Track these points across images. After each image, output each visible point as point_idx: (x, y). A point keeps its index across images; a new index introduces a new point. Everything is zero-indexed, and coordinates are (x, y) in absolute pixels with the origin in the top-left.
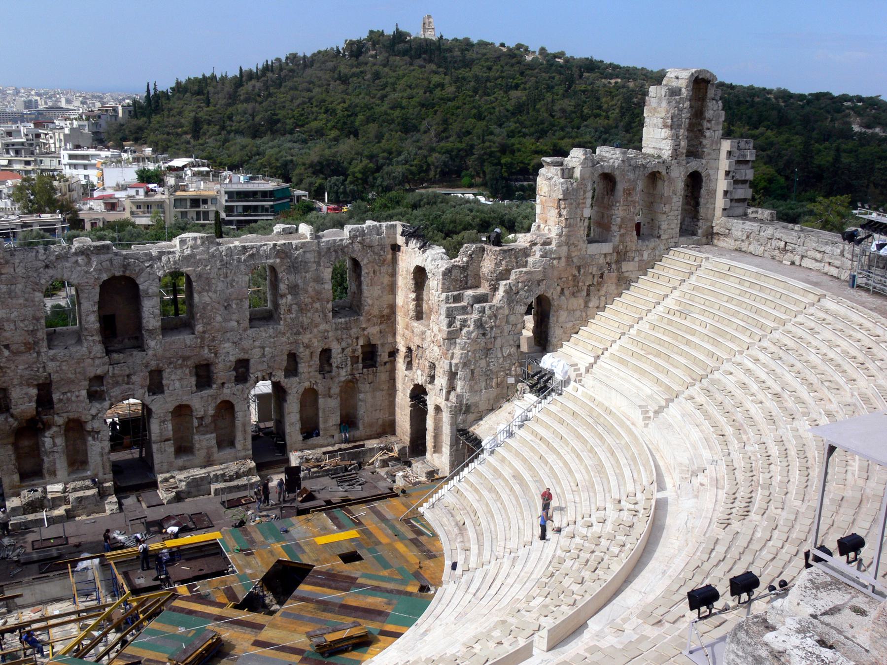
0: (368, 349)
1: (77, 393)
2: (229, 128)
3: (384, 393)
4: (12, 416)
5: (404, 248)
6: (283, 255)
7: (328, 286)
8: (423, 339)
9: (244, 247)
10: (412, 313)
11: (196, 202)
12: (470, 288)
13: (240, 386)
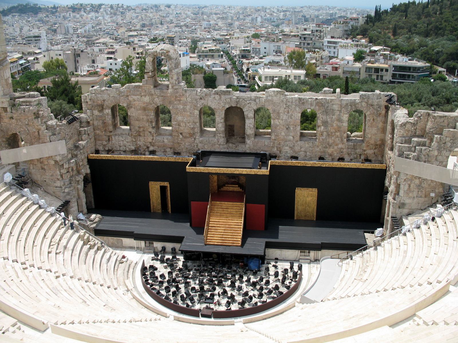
2: (413, 31)
6: (320, 105)
7: (345, 124)
11: (377, 70)
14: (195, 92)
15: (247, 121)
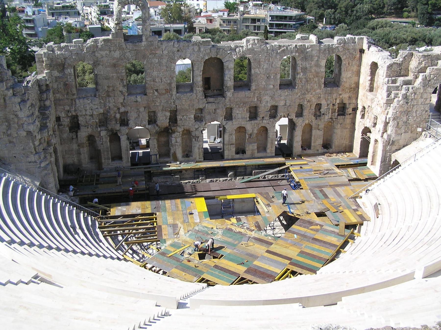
0: (342, 106)
1: (189, 116)
3: (348, 130)
4: (157, 125)
5: (366, 51)
7: (323, 70)
8: (372, 103)
9: (280, 46)
10: (368, 88)
11: (254, 20)
12: (402, 76)
13: (271, 120)
14: (172, 44)
15: (226, 72)
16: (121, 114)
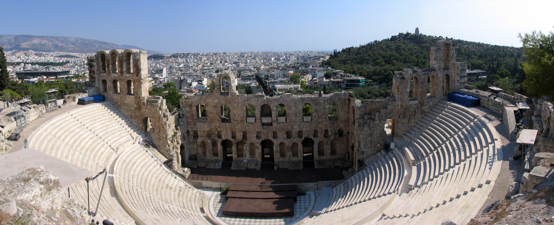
16: (218, 132)
